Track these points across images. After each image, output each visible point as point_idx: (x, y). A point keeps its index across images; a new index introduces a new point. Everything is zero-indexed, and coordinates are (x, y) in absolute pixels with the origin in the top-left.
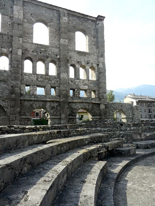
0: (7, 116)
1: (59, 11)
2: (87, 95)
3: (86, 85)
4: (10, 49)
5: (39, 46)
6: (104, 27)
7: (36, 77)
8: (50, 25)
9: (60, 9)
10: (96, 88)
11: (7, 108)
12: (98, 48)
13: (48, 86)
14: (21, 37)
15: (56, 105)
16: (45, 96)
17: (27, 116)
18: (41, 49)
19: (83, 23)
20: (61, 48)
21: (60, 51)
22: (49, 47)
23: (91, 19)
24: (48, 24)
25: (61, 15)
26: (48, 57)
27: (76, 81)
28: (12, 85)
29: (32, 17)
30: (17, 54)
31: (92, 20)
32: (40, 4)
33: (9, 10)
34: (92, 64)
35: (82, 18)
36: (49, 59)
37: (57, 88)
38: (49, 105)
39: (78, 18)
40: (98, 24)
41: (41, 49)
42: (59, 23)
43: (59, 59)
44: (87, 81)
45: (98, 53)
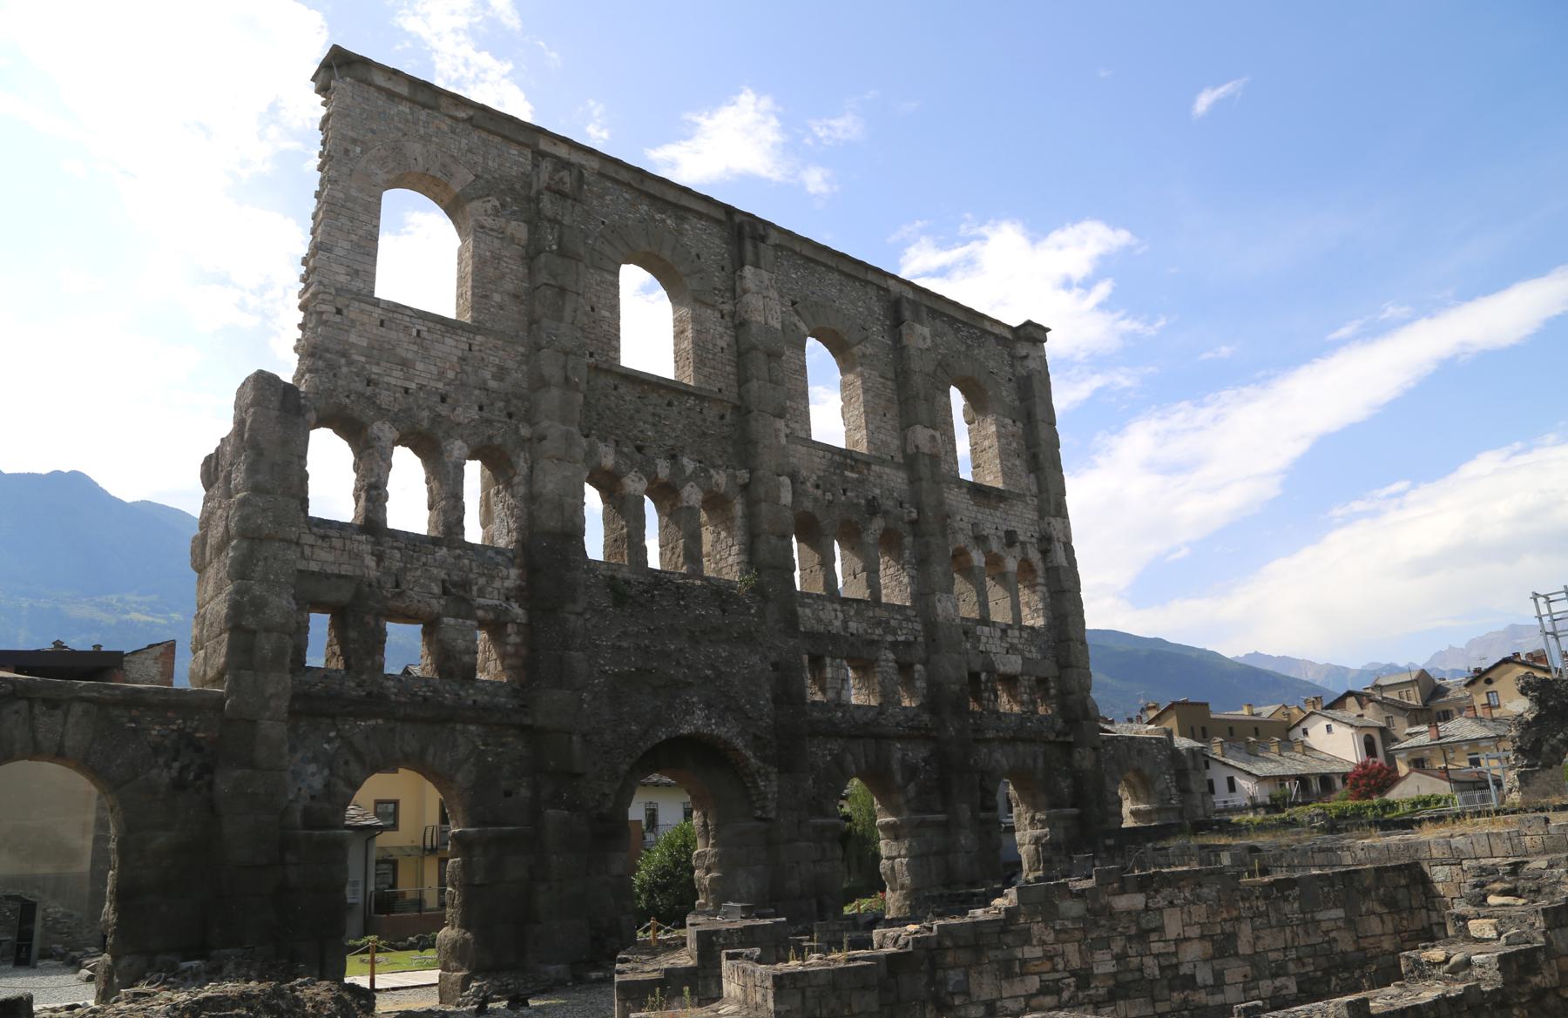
0: (760, 819)
1: (887, 290)
2: (1022, 703)
3: (1012, 649)
4: (743, 475)
5: (837, 458)
7: (840, 615)
8: (864, 355)
9: (891, 283)
10: (1049, 669)
11: (767, 777)
13: (887, 660)
14: (781, 416)
15: (918, 753)
16: (881, 709)
17: (826, 816)
18: (847, 473)
19: (968, 347)
20: (924, 470)
21: (914, 480)
22: (868, 464)
23: (997, 330)
24: (855, 350)
25: (907, 314)
28: (773, 656)
29: (797, 313)
30: (776, 501)
31: (999, 339)
32: (822, 258)
33: (718, 280)
34: (1023, 544)
35: (964, 324)
36: (878, 524)
37: (918, 667)
38: (899, 755)
39: (951, 326)
40: (1026, 357)
41: (847, 473)
42: (899, 348)
43: (913, 523)
44: (1017, 633)
45: (1040, 491)
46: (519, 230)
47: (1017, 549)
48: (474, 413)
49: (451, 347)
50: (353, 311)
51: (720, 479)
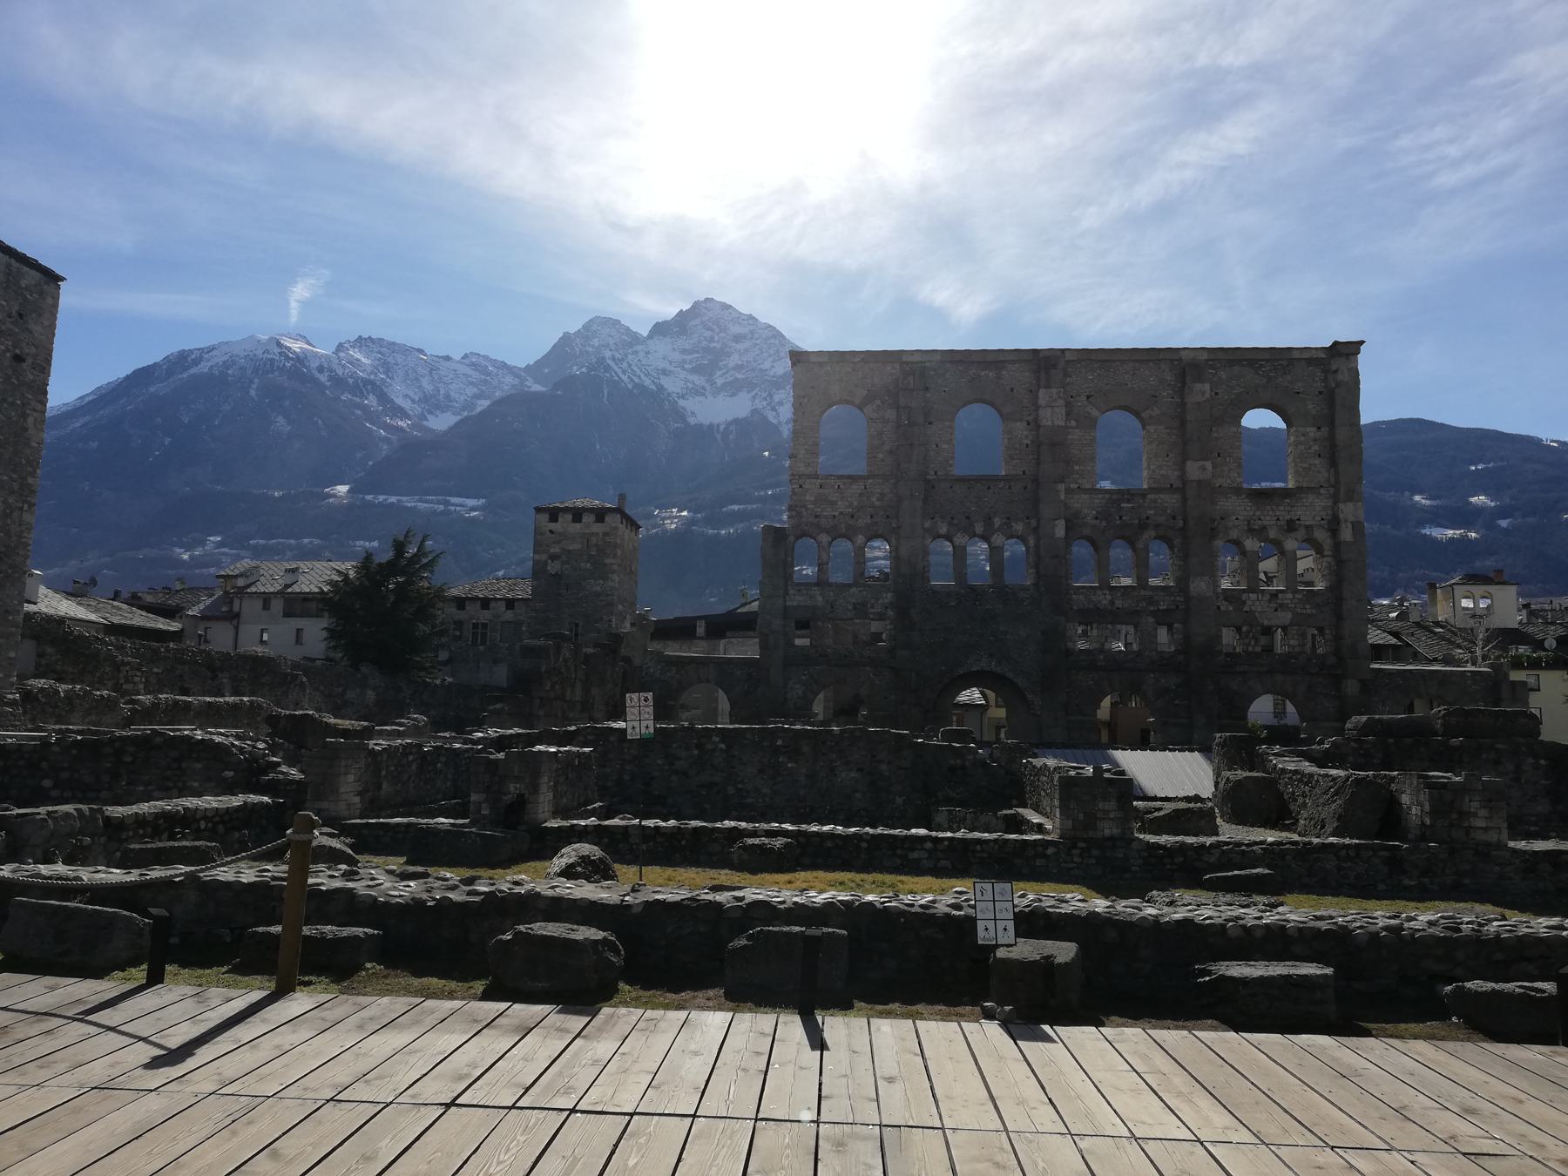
4: (1034, 523)
6: (1358, 382)
12: (1333, 463)
14: (1062, 481)
21: (1185, 500)
23: (1306, 355)
26: (1143, 526)
27: (1244, 596)
31: (1310, 361)
42: (1183, 404)
46: (890, 414)
47: (1301, 533)
48: (868, 520)
49: (857, 488)
50: (806, 486)
51: (1019, 527)
